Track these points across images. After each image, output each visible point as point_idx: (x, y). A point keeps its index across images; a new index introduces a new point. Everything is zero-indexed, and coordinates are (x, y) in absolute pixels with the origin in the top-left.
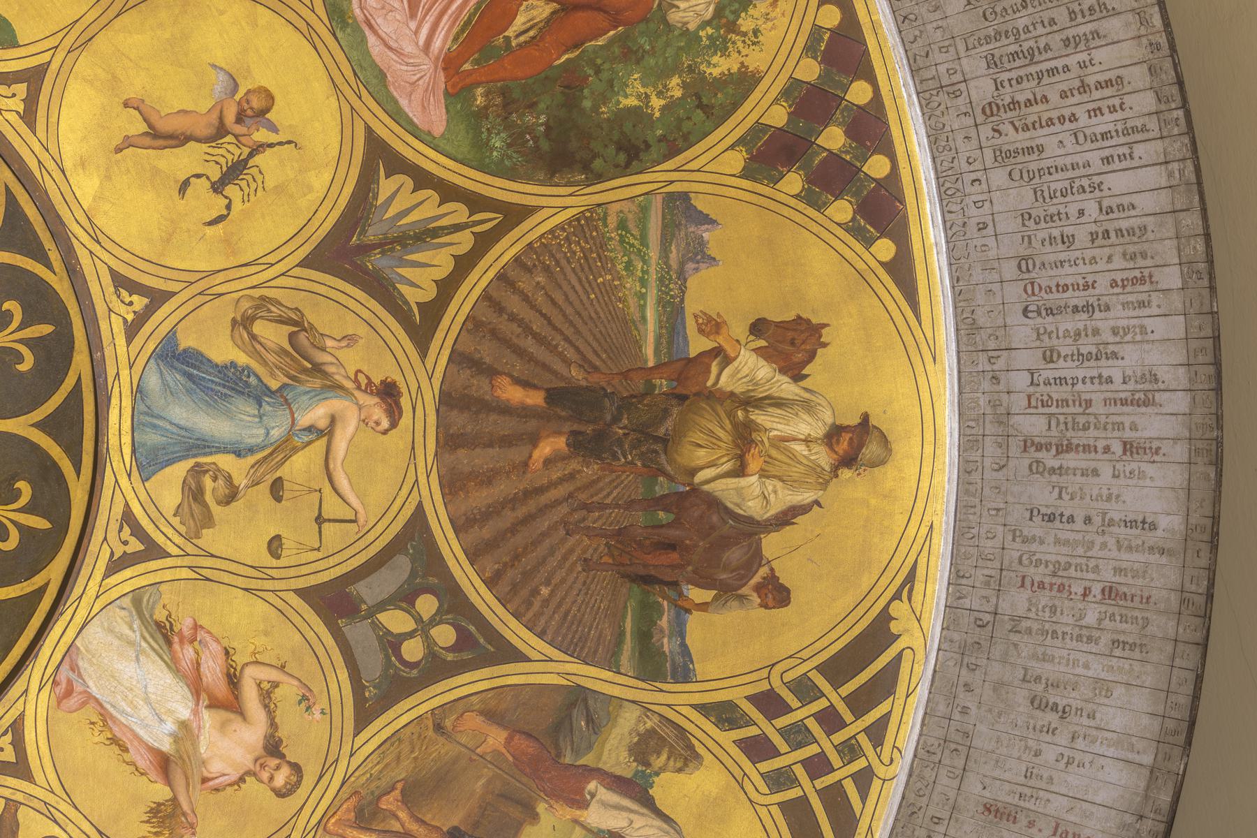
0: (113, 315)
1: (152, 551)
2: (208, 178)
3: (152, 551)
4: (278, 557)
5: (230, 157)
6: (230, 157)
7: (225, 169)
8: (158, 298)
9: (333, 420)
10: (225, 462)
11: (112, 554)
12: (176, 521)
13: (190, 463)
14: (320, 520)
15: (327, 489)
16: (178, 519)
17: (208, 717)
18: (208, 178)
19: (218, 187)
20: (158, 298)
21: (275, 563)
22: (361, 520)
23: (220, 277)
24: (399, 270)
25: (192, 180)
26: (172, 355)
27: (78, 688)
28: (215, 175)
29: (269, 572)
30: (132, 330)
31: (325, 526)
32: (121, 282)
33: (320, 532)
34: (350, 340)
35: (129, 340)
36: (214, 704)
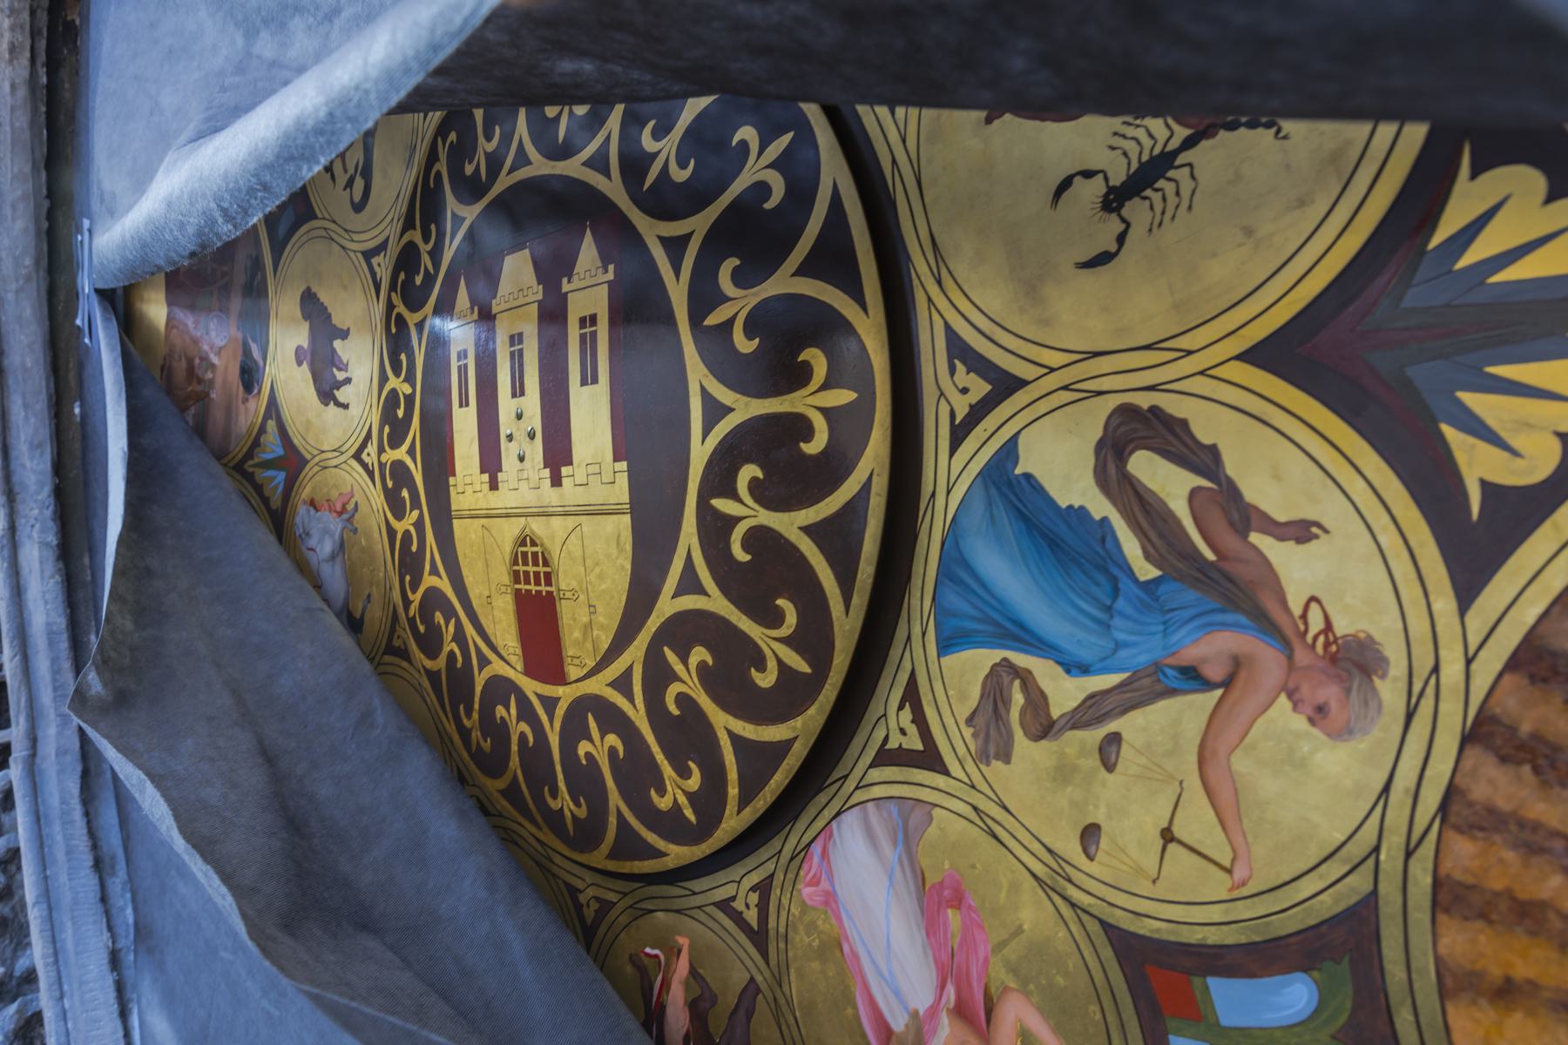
0: (943, 401)
1: (930, 759)
2: (1106, 179)
3: (930, 759)
4: (1091, 859)
5: (1147, 143)
6: (1147, 143)
7: (1135, 165)
8: (1005, 385)
9: (1237, 665)
10: (1044, 671)
11: (886, 739)
12: (968, 732)
13: (997, 655)
14: (1168, 836)
15: (1193, 782)
16: (971, 730)
17: (946, 1025)
18: (1106, 179)
19: (1114, 200)
20: (1005, 385)
21: (1082, 861)
22: (1239, 874)
23: (1104, 364)
24: (1467, 398)
25: (1147, 202)
26: (1006, 483)
27: (825, 885)
28: (1117, 179)
29: (1068, 869)
30: (959, 434)
31: (1172, 847)
32: (959, 350)
33: (1164, 849)
34: (1302, 532)
35: (955, 446)
36: (961, 1011)
